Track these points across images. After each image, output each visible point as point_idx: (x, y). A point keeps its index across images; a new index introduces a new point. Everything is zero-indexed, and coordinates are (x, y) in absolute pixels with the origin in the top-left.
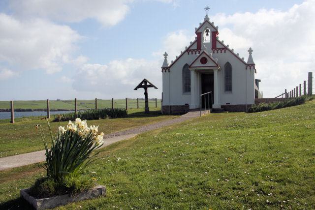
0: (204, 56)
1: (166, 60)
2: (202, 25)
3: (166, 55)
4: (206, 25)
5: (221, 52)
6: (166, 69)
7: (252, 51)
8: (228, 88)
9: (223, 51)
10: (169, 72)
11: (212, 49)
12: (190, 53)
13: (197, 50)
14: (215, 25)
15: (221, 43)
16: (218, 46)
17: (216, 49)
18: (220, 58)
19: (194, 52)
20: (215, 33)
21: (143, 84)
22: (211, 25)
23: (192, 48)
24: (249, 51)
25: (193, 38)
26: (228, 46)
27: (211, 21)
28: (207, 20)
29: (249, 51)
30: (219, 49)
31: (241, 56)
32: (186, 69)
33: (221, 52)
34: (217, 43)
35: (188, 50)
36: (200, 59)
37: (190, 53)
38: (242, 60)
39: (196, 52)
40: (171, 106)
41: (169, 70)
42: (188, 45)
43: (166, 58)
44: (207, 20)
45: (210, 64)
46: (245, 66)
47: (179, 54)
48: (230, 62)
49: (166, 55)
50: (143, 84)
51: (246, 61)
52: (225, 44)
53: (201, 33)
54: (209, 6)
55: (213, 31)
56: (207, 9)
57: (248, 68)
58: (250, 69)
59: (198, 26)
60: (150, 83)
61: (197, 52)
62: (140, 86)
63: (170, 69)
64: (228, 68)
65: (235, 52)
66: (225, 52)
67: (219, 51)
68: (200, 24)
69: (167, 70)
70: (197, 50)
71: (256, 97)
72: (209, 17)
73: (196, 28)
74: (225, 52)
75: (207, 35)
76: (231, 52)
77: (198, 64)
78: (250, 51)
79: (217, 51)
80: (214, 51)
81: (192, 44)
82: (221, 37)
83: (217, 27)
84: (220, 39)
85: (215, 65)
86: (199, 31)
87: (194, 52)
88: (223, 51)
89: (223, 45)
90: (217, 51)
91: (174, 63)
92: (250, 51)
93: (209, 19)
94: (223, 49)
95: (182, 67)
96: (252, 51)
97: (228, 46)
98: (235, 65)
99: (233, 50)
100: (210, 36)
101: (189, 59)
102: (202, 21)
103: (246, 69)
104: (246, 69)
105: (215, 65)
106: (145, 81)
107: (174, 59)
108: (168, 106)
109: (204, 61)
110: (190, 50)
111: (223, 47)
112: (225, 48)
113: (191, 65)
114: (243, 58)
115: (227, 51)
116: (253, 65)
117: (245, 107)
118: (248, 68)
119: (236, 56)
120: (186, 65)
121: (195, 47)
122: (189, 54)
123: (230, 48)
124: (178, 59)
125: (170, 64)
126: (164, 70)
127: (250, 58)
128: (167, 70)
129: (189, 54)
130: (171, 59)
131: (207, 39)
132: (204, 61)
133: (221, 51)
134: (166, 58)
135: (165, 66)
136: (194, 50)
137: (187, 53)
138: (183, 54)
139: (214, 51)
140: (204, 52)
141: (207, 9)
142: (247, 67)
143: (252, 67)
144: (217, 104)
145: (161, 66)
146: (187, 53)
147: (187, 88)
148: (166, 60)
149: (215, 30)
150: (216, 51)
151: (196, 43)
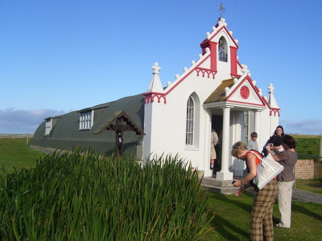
10: (165, 102)
12: (201, 73)
13: (211, 71)
19: (206, 74)
23: (201, 66)
32: (193, 98)
37: (201, 73)
39: (209, 74)
53: (216, 43)
55: (232, 45)
57: (273, 113)
61: (211, 75)
63: (167, 97)
69: (162, 99)
87: (206, 74)
103: (271, 115)
104: (271, 115)
110: (201, 69)
118: (273, 113)
121: (207, 65)
122: (198, 75)
128: (162, 99)
129: (198, 75)
136: (206, 70)
137: (195, 72)
146: (195, 72)
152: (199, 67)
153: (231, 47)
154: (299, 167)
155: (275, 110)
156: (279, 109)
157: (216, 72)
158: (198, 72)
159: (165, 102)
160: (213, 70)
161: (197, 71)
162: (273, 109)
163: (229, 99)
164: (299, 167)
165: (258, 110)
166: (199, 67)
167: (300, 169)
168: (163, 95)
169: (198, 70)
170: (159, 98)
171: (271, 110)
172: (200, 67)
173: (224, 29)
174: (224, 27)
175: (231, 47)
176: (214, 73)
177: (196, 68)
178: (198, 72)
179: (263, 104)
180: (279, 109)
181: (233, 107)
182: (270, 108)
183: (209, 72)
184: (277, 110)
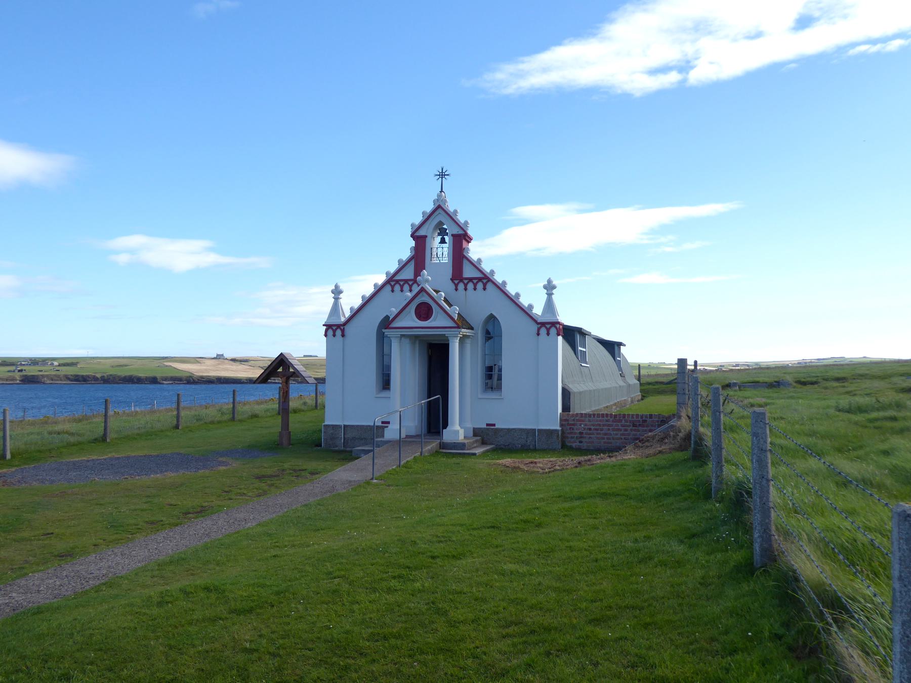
0: (424, 298)
2: (428, 218)
3: (337, 292)
4: (440, 217)
5: (475, 289)
6: (334, 329)
9: (480, 285)
10: (343, 335)
11: (452, 280)
12: (397, 287)
14: (461, 219)
15: (476, 266)
16: (468, 272)
17: (461, 280)
20: (461, 239)
22: (452, 217)
24: (545, 287)
26: (492, 272)
27: (451, 208)
28: (439, 207)
29: (545, 287)
30: (471, 280)
31: (524, 301)
33: (475, 289)
35: (392, 281)
37: (397, 287)
38: (526, 312)
40: (345, 426)
41: (343, 331)
42: (393, 268)
43: (337, 299)
44: (439, 207)
45: (438, 321)
46: (535, 327)
48: (495, 314)
49: (337, 292)
50: (280, 370)
51: (538, 310)
52: (486, 267)
53: (426, 237)
54: (449, 169)
55: (455, 232)
56: (442, 175)
57: (543, 331)
58: (548, 334)
59: (418, 220)
63: (347, 328)
65: (511, 290)
66: (484, 289)
69: (339, 332)
71: (566, 408)
73: (412, 225)
74: (484, 289)
75: (443, 241)
76: (501, 289)
77: (410, 320)
78: (550, 287)
79: (466, 285)
80: (456, 285)
81: (403, 266)
82: (474, 250)
83: (466, 223)
85: (454, 325)
86: (421, 233)
88: (480, 285)
90: (466, 285)
91: (356, 313)
92: (550, 287)
94: (480, 279)
96: (554, 287)
97: (492, 272)
99: (504, 283)
100: (447, 245)
101: (391, 304)
102: (429, 208)
103: (538, 334)
104: (538, 334)
105: (452, 324)
107: (358, 303)
108: (340, 426)
109: (424, 312)
110: (397, 282)
111: (479, 275)
112: (485, 280)
114: (531, 307)
115: (489, 285)
118: (543, 331)
119: (513, 301)
120: (387, 317)
121: (408, 274)
122: (393, 291)
123: (498, 278)
124: (367, 302)
125: (348, 314)
126: (330, 332)
127: (550, 305)
128: (339, 332)
129: (393, 291)
130: (351, 301)
131: (440, 254)
132: (424, 312)
133: (475, 285)
134: (337, 299)
135: (335, 321)
136: (406, 281)
137: (388, 288)
138: (379, 290)
139: (456, 285)
140: (423, 290)
141: (442, 175)
142: (539, 329)
145: (324, 319)
146: (388, 288)
148: (336, 308)
149: (461, 232)
150: (461, 286)
151: (413, 262)
154: (630, 428)
155: (548, 326)
158: (393, 287)
159: (343, 335)
161: (391, 285)
162: (543, 324)
163: (394, 325)
164: (629, 428)
165: (446, 335)
167: (634, 432)
168: (338, 326)
169: (393, 283)
170: (334, 332)
171: (539, 326)
172: (397, 278)
173: (440, 211)
174: (439, 207)
178: (393, 287)
179: (456, 325)
181: (399, 336)
182: (538, 323)
183: (411, 283)
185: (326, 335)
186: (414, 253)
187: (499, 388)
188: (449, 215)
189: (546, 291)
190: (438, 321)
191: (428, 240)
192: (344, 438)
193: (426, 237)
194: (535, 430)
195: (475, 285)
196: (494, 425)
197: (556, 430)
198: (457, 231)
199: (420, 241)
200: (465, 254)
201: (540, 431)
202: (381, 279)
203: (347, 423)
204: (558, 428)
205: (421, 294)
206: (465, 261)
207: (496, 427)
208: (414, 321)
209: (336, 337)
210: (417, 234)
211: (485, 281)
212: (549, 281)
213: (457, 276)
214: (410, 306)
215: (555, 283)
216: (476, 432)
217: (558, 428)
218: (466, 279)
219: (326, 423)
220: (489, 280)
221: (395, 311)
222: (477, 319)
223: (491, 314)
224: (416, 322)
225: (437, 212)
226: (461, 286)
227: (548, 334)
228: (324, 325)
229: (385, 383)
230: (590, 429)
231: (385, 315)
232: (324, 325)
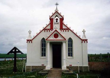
0: (56, 33)
1: (30, 36)
7: (85, 31)
8: (70, 54)
10: (32, 43)
11: (60, 29)
12: (46, 31)
13: (51, 29)
14: (62, 15)
16: (64, 27)
17: (62, 29)
18: (66, 35)
19: (48, 31)
20: (62, 19)
21: (14, 51)
25: (48, 22)
27: (59, 12)
28: (57, 12)
29: (83, 31)
30: (65, 29)
31: (78, 35)
34: (63, 25)
35: (45, 29)
36: (53, 35)
37: (46, 31)
39: (49, 31)
42: (45, 26)
44: (57, 12)
45: (59, 38)
47: (39, 32)
49: (30, 32)
50: (14, 51)
51: (81, 37)
52: (68, 26)
53: (53, 19)
54: (58, 3)
56: (57, 4)
57: (83, 42)
58: (85, 42)
59: (51, 15)
60: (18, 50)
61: (51, 31)
62: (11, 52)
63: (33, 41)
64: (70, 40)
65: (75, 32)
66: (68, 31)
67: (65, 31)
68: (52, 13)
70: (51, 29)
72: (58, 9)
73: (50, 16)
74: (68, 31)
78: (84, 31)
79: (63, 30)
83: (63, 16)
84: (65, 23)
86: (52, 18)
88: (67, 31)
89: (67, 27)
90: (63, 30)
92: (84, 31)
93: (58, 11)
94: (67, 29)
95: (41, 39)
98: (74, 39)
102: (54, 12)
104: (82, 42)
105: (64, 39)
106: (15, 48)
108: (30, 66)
109: (56, 36)
110: (46, 29)
111: (67, 28)
112: (68, 29)
113: (47, 39)
114: (80, 36)
115: (69, 31)
116: (86, 40)
117: (82, 68)
118: (83, 42)
120: (43, 39)
121: (49, 27)
122: (45, 32)
123: (71, 29)
125: (33, 38)
128: (30, 42)
129: (45, 32)
130: (34, 34)
132: (56, 36)
133: (66, 30)
136: (48, 29)
137: (44, 31)
140: (56, 30)
142: (82, 41)
143: (86, 42)
144: (64, 67)
147: (44, 54)
148: (30, 36)
150: (62, 31)
151: (50, 25)
152: (46, 28)
153: (60, 19)
156: (87, 40)
157: (53, 29)
158: (45, 31)
159: (32, 43)
160: (52, 28)
162: (83, 40)
166: (46, 28)
168: (31, 40)
170: (29, 42)
172: (46, 28)
173: (57, 13)
175: (60, 19)
176: (52, 30)
177: (44, 29)
178: (45, 31)
180: (87, 40)
184: (86, 40)
185: (27, 43)
186: (50, 23)
187: (72, 56)
188: (59, 14)
189: (83, 32)
190: (59, 38)
191: (54, 20)
192: (32, 69)
193: (53, 19)
194: (82, 66)
195: (66, 30)
196: (71, 65)
197: (88, 67)
198: (61, 18)
199: (51, 20)
200: (63, 23)
201: (84, 67)
202: (42, 29)
203: (32, 65)
204: (88, 66)
205: (55, 32)
206: (63, 25)
207: (72, 66)
208: (53, 38)
209: (30, 43)
210: (51, 18)
211: (68, 30)
212: (84, 30)
213: (61, 28)
214: (52, 35)
215: (85, 30)
216: (67, 67)
217: (88, 66)
218: (64, 29)
219: (27, 65)
220: (69, 29)
221: (48, 36)
222: (67, 39)
223: (70, 38)
224: (53, 38)
225: (56, 13)
226: (62, 31)
227: (85, 42)
228: (27, 40)
229: (44, 54)
230: (96, 66)
231: (43, 38)
232: (27, 40)
